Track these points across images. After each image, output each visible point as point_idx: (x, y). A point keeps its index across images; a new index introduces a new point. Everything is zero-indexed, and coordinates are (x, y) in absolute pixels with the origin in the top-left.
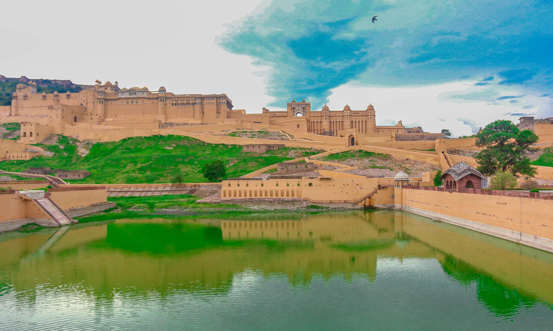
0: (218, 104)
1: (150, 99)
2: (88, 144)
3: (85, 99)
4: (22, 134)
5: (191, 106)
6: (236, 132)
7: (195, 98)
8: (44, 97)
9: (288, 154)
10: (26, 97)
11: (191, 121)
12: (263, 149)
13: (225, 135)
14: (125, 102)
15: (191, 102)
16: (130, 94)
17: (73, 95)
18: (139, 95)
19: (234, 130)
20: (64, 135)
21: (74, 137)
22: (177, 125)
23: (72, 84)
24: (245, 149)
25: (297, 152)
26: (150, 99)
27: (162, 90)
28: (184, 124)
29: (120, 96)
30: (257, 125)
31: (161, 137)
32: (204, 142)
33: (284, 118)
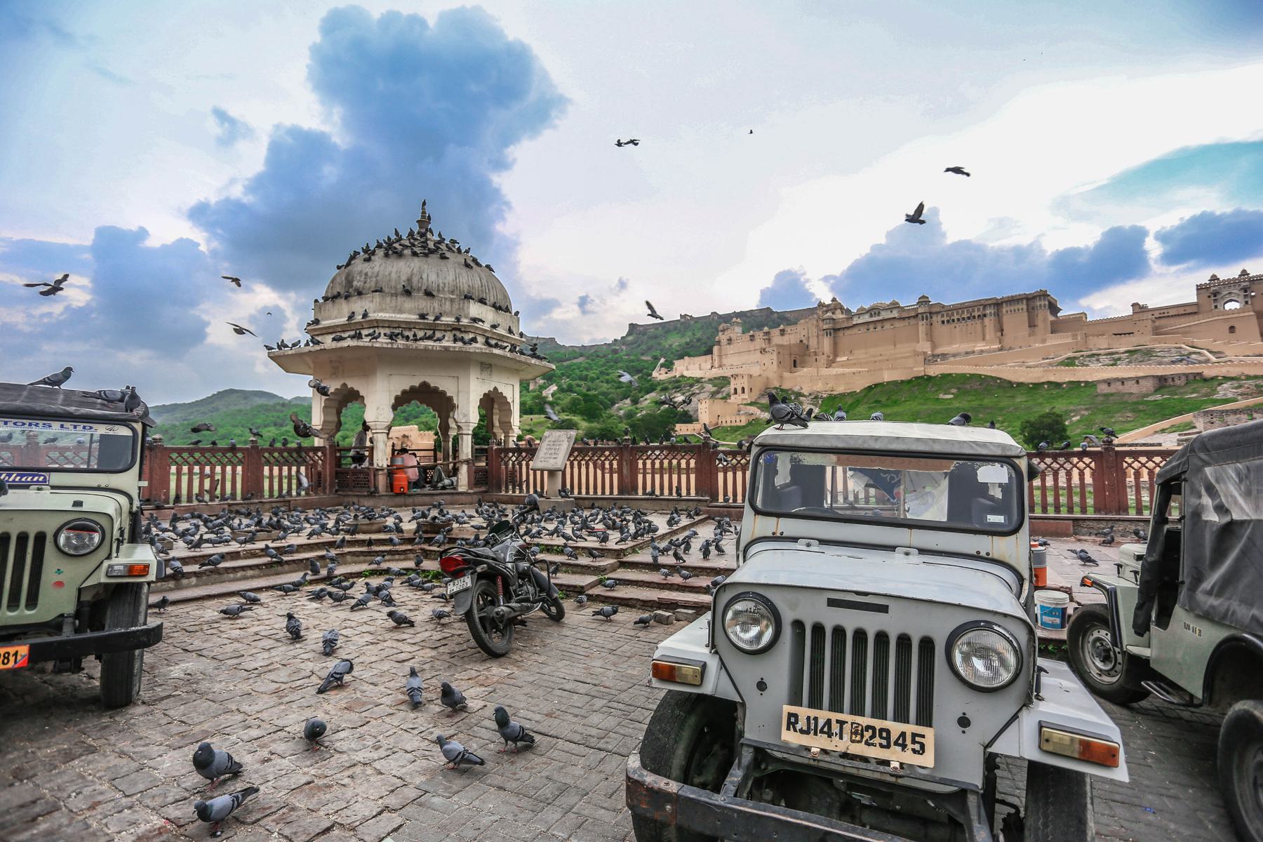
0: (1031, 311)
2: (816, 397)
3: (805, 333)
5: (978, 322)
6: (1075, 358)
7: (985, 306)
8: (752, 338)
9: (1214, 391)
10: (730, 340)
11: (980, 346)
12: (1148, 385)
13: (1050, 364)
14: (863, 329)
15: (976, 314)
17: (788, 329)
18: (885, 315)
19: (1070, 354)
20: (784, 387)
21: (796, 389)
22: (954, 356)
23: (772, 312)
24: (1103, 388)
25: (1240, 387)
27: (924, 301)
28: (967, 353)
29: (856, 321)
30: (1124, 339)
31: (930, 378)
32: (1010, 382)
33: (1191, 318)
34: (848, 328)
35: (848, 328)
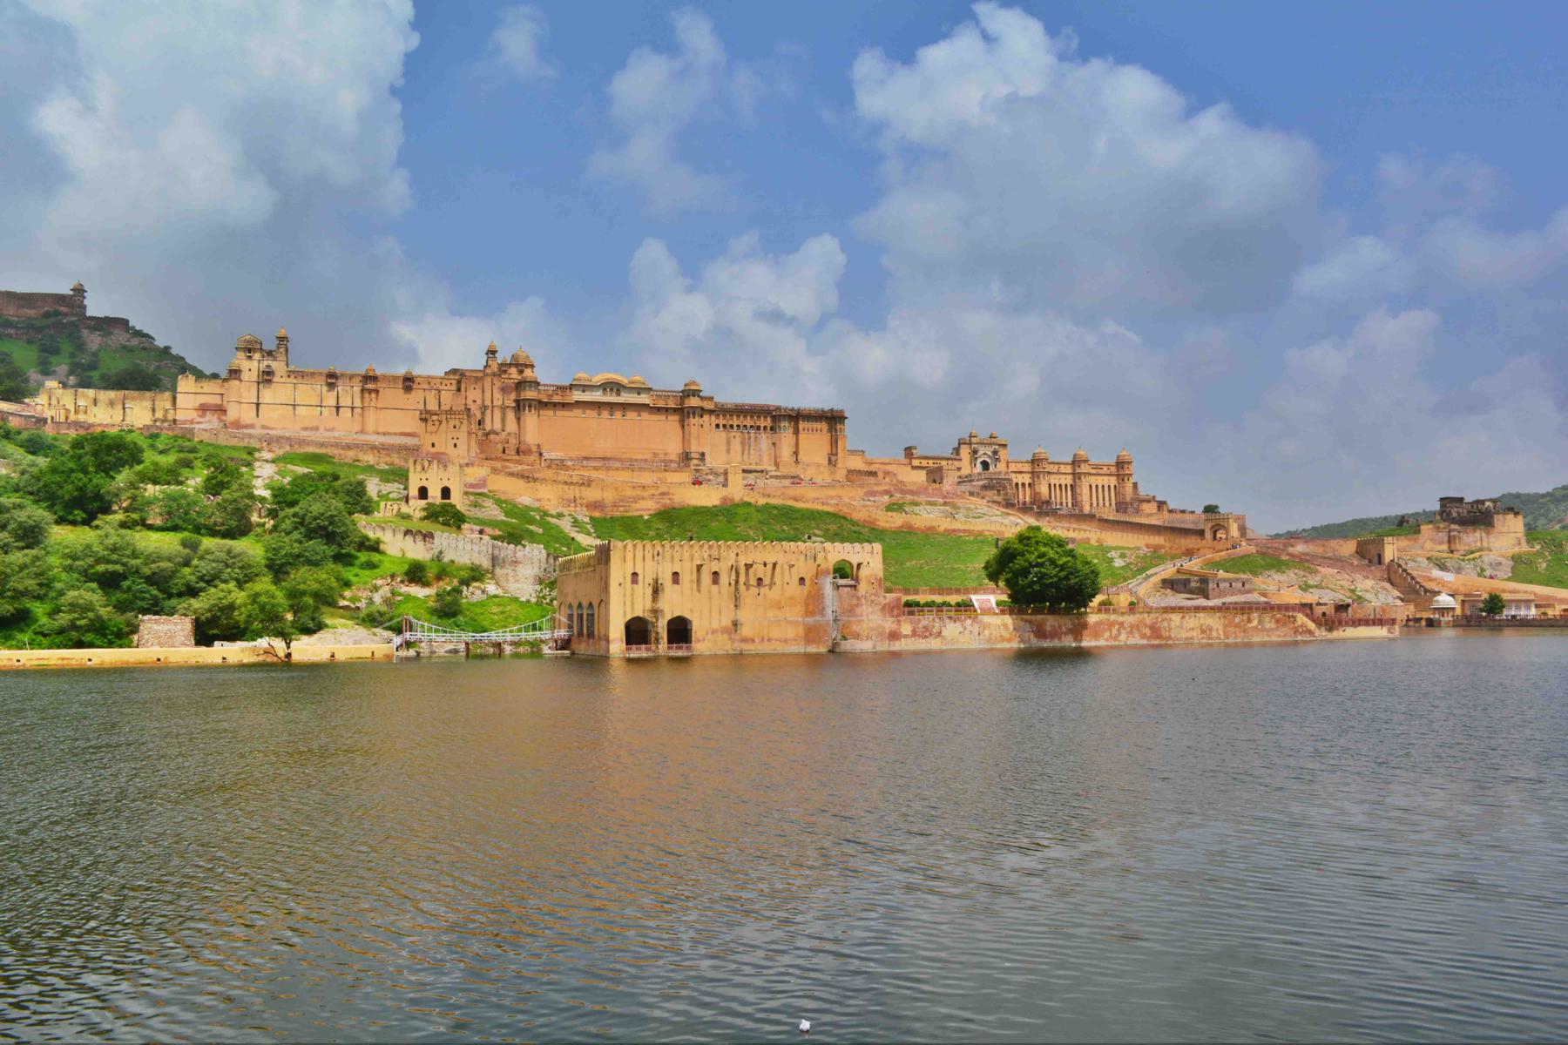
1: (659, 409)
4: (414, 492)
26: (659, 410)
34: (564, 406)
35: (564, 406)
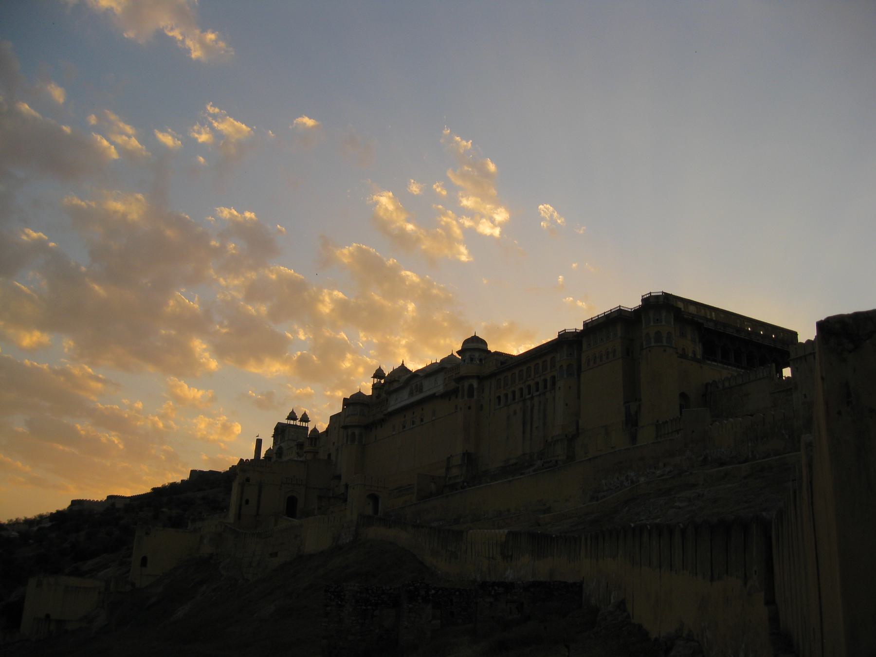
16: (411, 394)
